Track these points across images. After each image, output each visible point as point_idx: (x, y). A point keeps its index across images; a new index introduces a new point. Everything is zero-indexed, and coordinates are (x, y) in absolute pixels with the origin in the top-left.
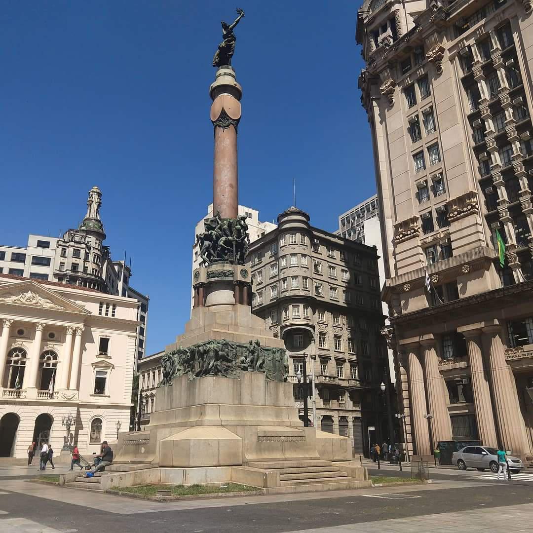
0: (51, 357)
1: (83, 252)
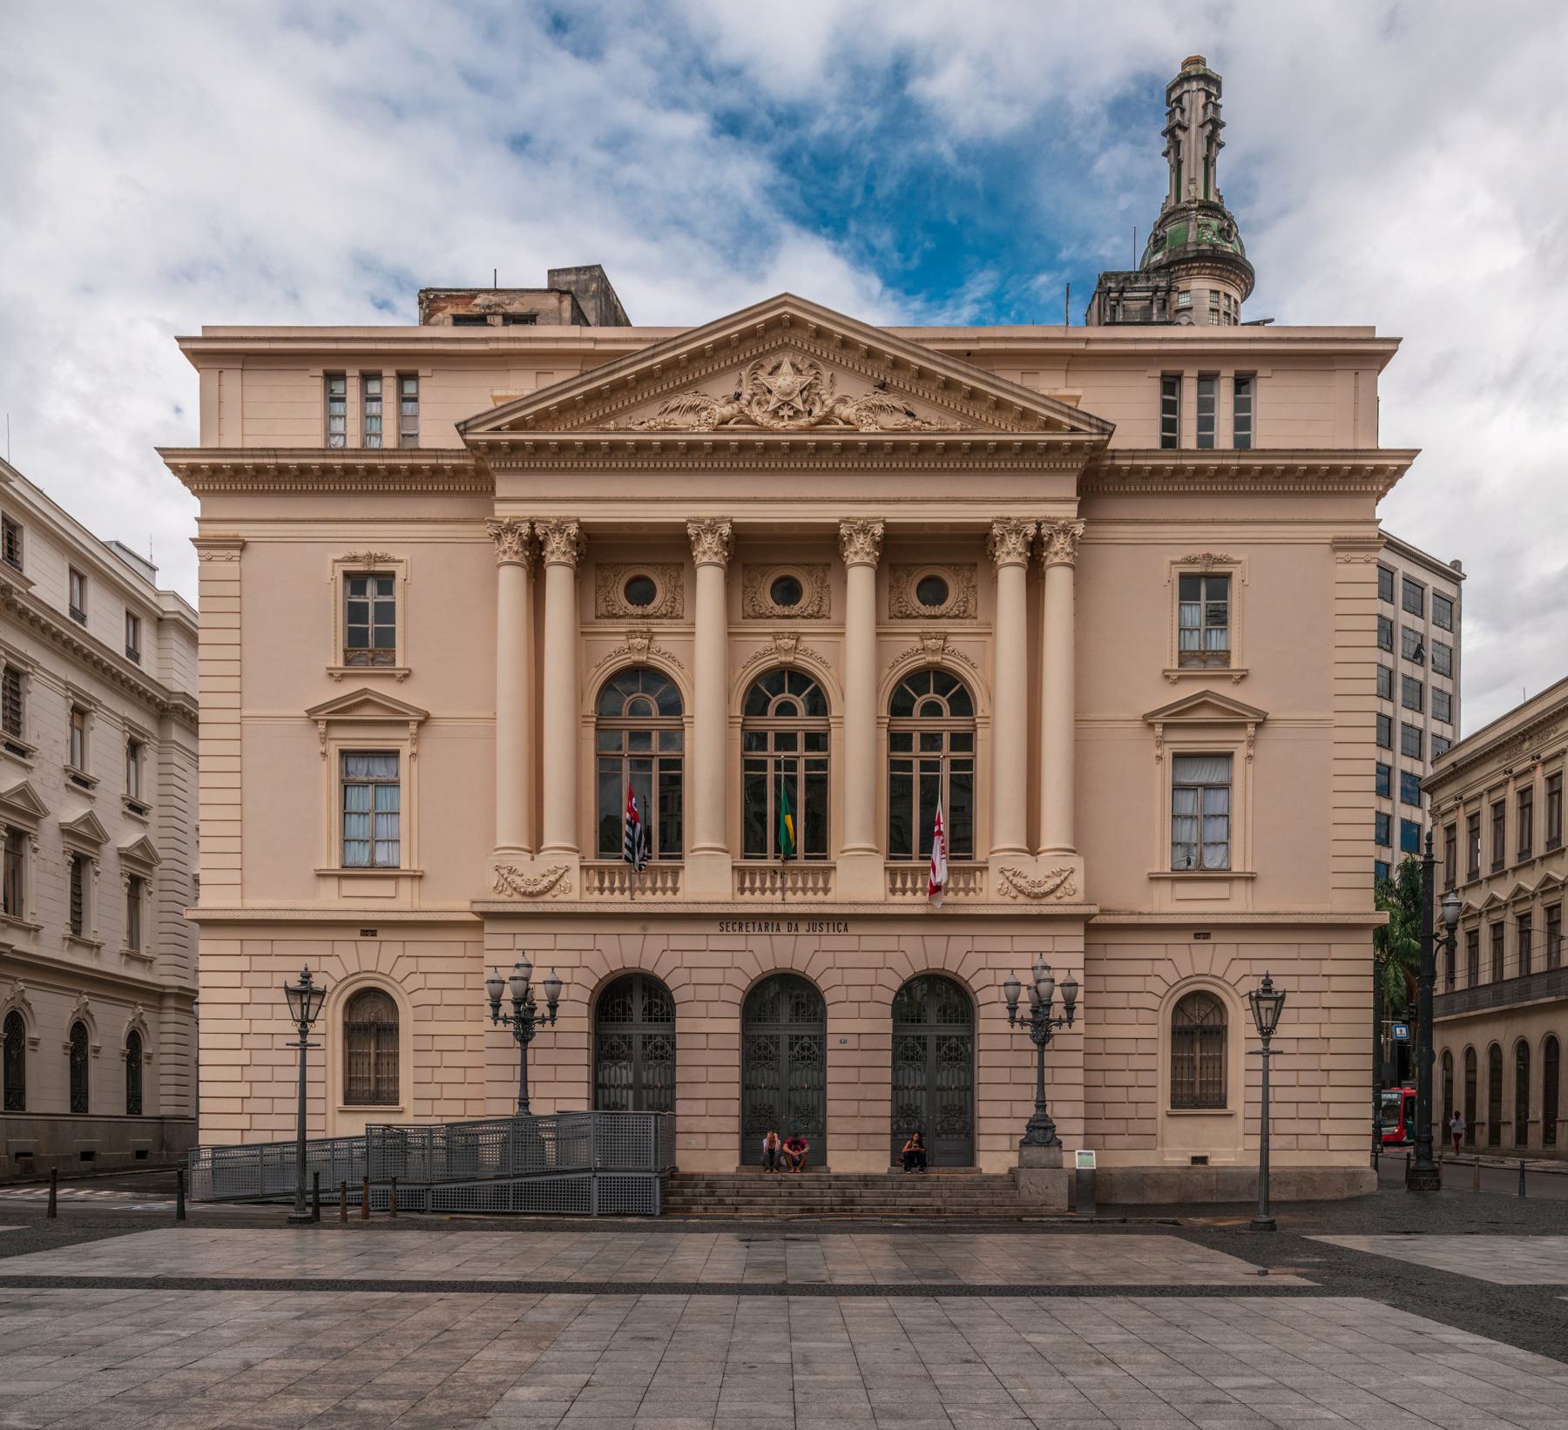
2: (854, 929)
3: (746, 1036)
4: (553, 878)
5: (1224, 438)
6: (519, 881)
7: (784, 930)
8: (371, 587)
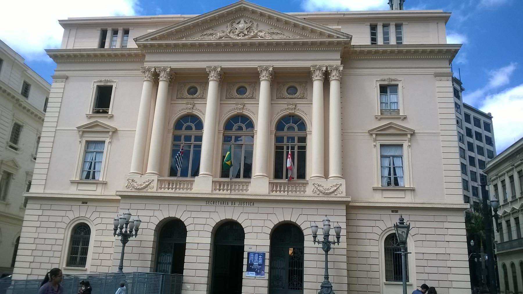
0: (296, 126)
2: (256, 205)
4: (147, 184)
5: (393, 41)
6: (135, 184)
7: (230, 204)
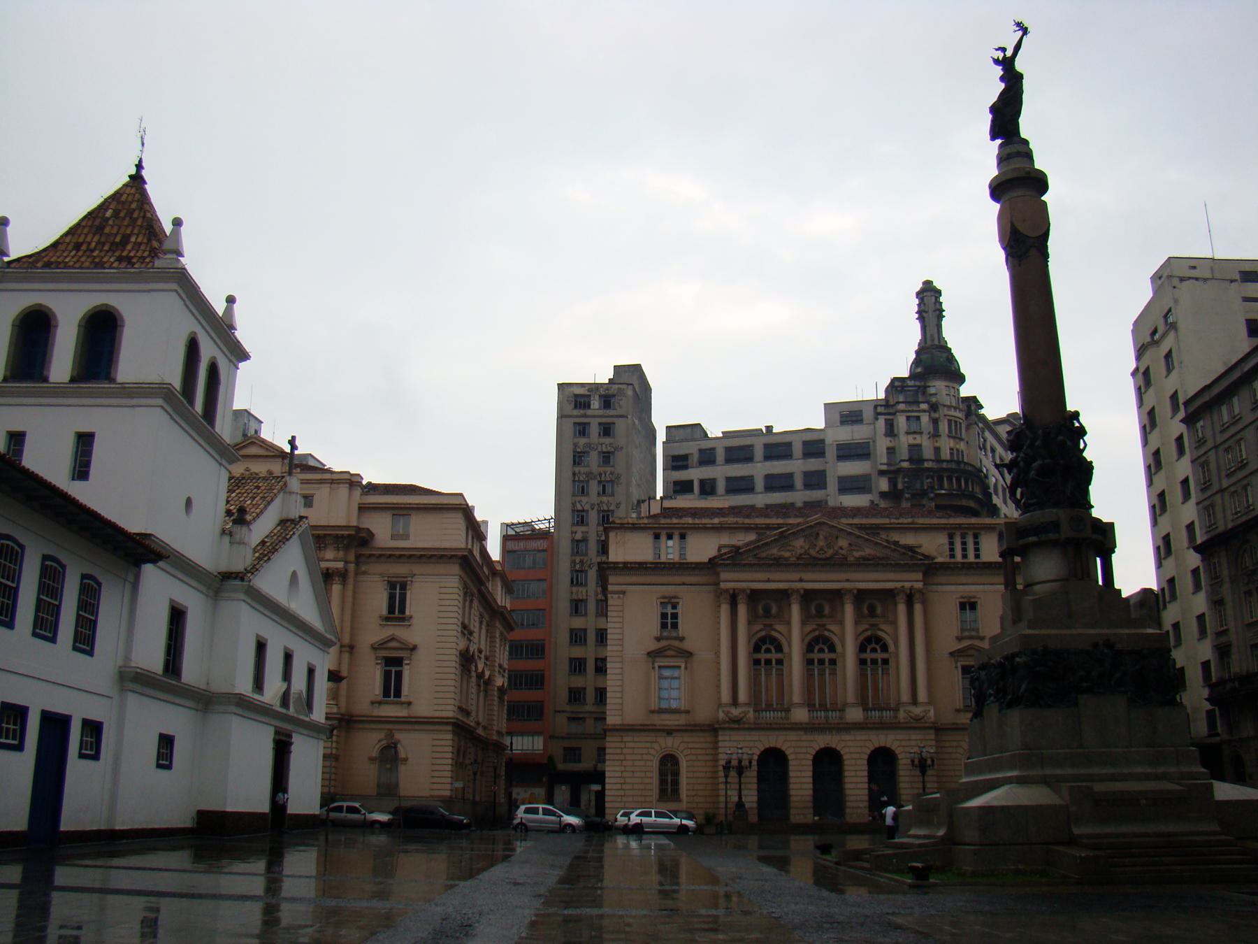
1: (925, 419)
3: (814, 772)
8: (669, 607)
